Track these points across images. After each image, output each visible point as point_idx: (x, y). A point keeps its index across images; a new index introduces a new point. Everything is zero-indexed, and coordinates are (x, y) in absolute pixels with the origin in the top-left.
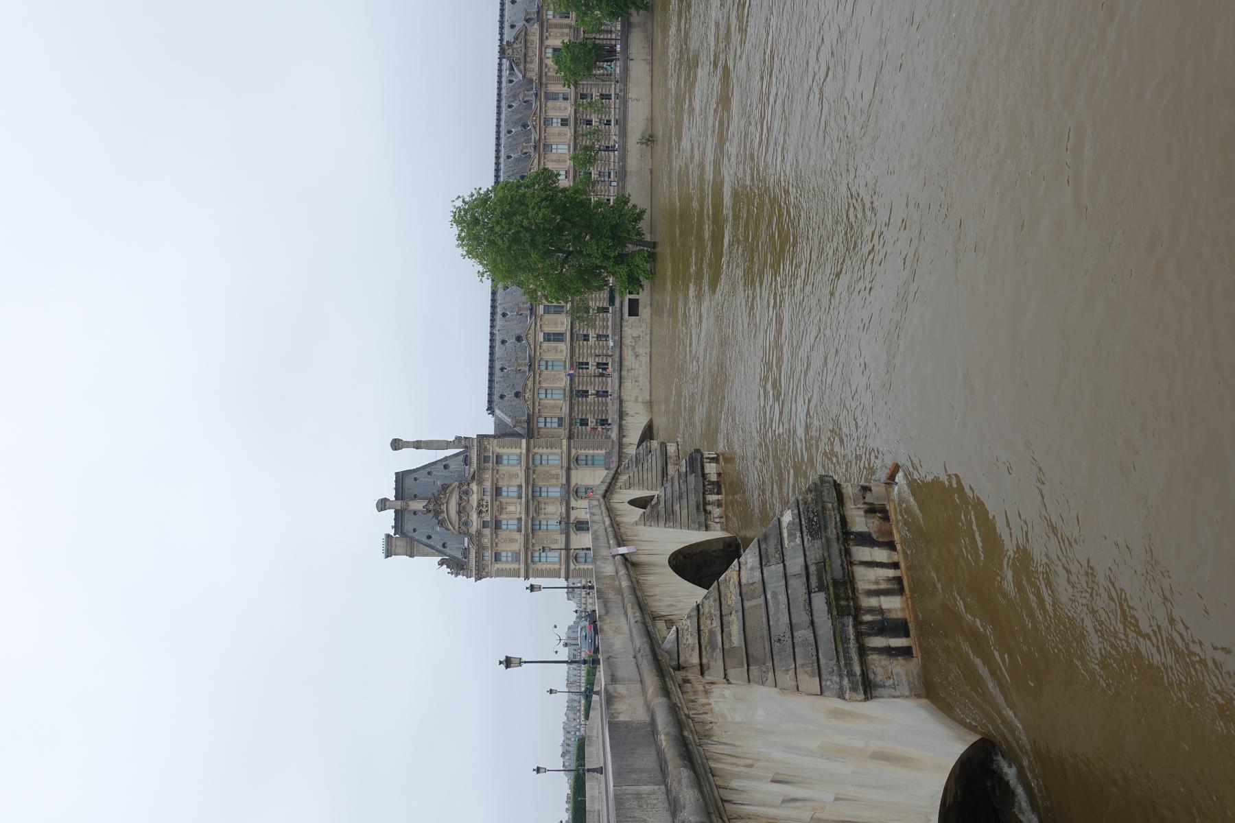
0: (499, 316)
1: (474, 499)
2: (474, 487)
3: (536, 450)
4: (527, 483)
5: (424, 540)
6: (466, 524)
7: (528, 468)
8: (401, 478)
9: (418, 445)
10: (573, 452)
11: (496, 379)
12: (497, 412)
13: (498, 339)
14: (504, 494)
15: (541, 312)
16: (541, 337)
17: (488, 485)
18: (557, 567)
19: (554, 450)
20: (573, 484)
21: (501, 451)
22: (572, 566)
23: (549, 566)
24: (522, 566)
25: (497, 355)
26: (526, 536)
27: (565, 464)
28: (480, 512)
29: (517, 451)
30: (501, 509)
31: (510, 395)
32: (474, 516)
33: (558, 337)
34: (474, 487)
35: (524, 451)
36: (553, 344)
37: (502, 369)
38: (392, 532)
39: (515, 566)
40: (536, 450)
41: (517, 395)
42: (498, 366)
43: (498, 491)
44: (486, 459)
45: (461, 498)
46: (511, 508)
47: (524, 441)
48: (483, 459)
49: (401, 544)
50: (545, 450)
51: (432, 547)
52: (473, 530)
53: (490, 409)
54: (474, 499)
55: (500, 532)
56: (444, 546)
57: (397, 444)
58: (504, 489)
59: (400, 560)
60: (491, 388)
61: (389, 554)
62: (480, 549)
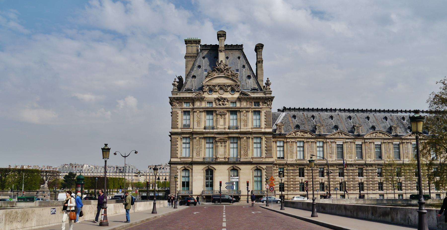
0: (348, 114)
1: (227, 95)
2: (237, 95)
3: (264, 139)
4: (241, 133)
5: (197, 64)
6: (211, 90)
7: (251, 133)
8: (239, 48)
9: (259, 62)
10: (264, 167)
11: (305, 113)
12: (284, 114)
13: (333, 114)
14: (231, 117)
15: (357, 143)
16: (340, 142)
17: (238, 105)
18: (179, 156)
19: (264, 152)
20: (240, 166)
21: (263, 114)
22: (179, 167)
23: (179, 149)
24: (179, 130)
25: (322, 113)
26: (202, 133)
27: (255, 160)
28: (218, 100)
29: (263, 126)
30: (222, 115)
31: (296, 122)
32: (215, 95)
33: (342, 155)
34: (237, 95)
35: (263, 130)
36: (335, 151)
37: (313, 117)
38: (202, 43)
39: (179, 126)
40: (264, 139)
41: (298, 126)
42: (315, 114)
43: (234, 112)
44: (257, 103)
45: (229, 86)
46: (221, 121)
47: (270, 130)
48: (257, 101)
49: (194, 49)
50: (264, 145)
51: (192, 69)
52: (206, 95)
53: (285, 109)
54: (227, 95)
55: (203, 114)
56: (194, 77)
57: (259, 48)
58: (235, 117)
59: (183, 50)
60: (299, 109)
61: (187, 42)
62: (192, 100)
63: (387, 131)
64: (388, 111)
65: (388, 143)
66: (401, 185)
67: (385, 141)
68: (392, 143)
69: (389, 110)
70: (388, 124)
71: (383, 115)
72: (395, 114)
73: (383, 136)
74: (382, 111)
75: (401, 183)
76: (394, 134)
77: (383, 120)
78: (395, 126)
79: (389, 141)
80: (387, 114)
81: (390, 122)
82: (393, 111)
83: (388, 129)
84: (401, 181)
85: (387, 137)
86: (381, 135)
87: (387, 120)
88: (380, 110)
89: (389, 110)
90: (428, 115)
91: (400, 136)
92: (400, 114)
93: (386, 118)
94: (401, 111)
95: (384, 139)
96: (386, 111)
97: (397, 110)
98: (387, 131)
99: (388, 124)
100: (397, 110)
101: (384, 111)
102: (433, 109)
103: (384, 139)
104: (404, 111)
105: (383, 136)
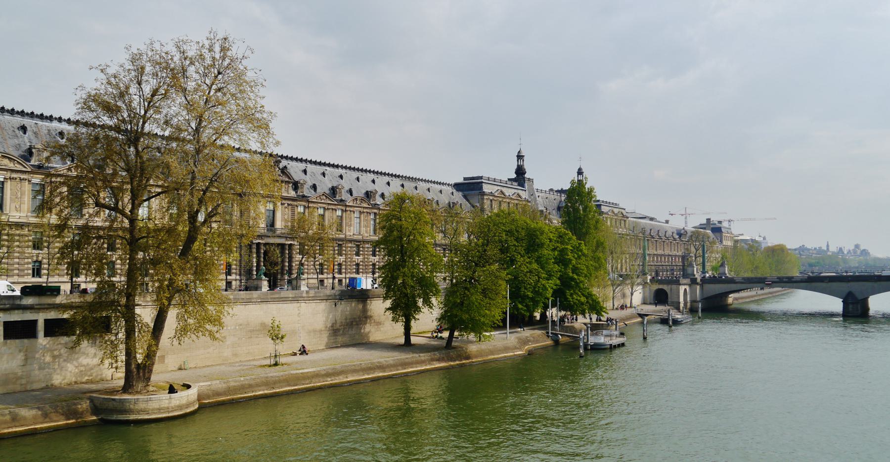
63: (22, 157)
64: (32, 115)
65: (21, 179)
66: (40, 266)
67: (14, 175)
68: (29, 181)
69: (32, 113)
70: (26, 140)
71: (19, 120)
72: (46, 124)
73: (11, 165)
74: (18, 113)
75: (40, 262)
76: (36, 164)
77: (17, 131)
78: (39, 146)
79: (23, 176)
80: (27, 121)
81: (32, 137)
82: (41, 117)
83: (25, 151)
84: (40, 259)
85: (20, 168)
86: (6, 161)
87: (25, 133)
88: (13, 110)
89: (32, 113)
90: (71, 128)
91: (48, 168)
92: (55, 124)
93: (24, 129)
94: (60, 120)
95: (13, 171)
96: (27, 114)
97: (51, 116)
98: (22, 157)
99: (27, 141)
100: (51, 116)
101: (22, 114)
102: (89, 116)
103: (13, 171)
104: (65, 120)
105: (11, 165)
